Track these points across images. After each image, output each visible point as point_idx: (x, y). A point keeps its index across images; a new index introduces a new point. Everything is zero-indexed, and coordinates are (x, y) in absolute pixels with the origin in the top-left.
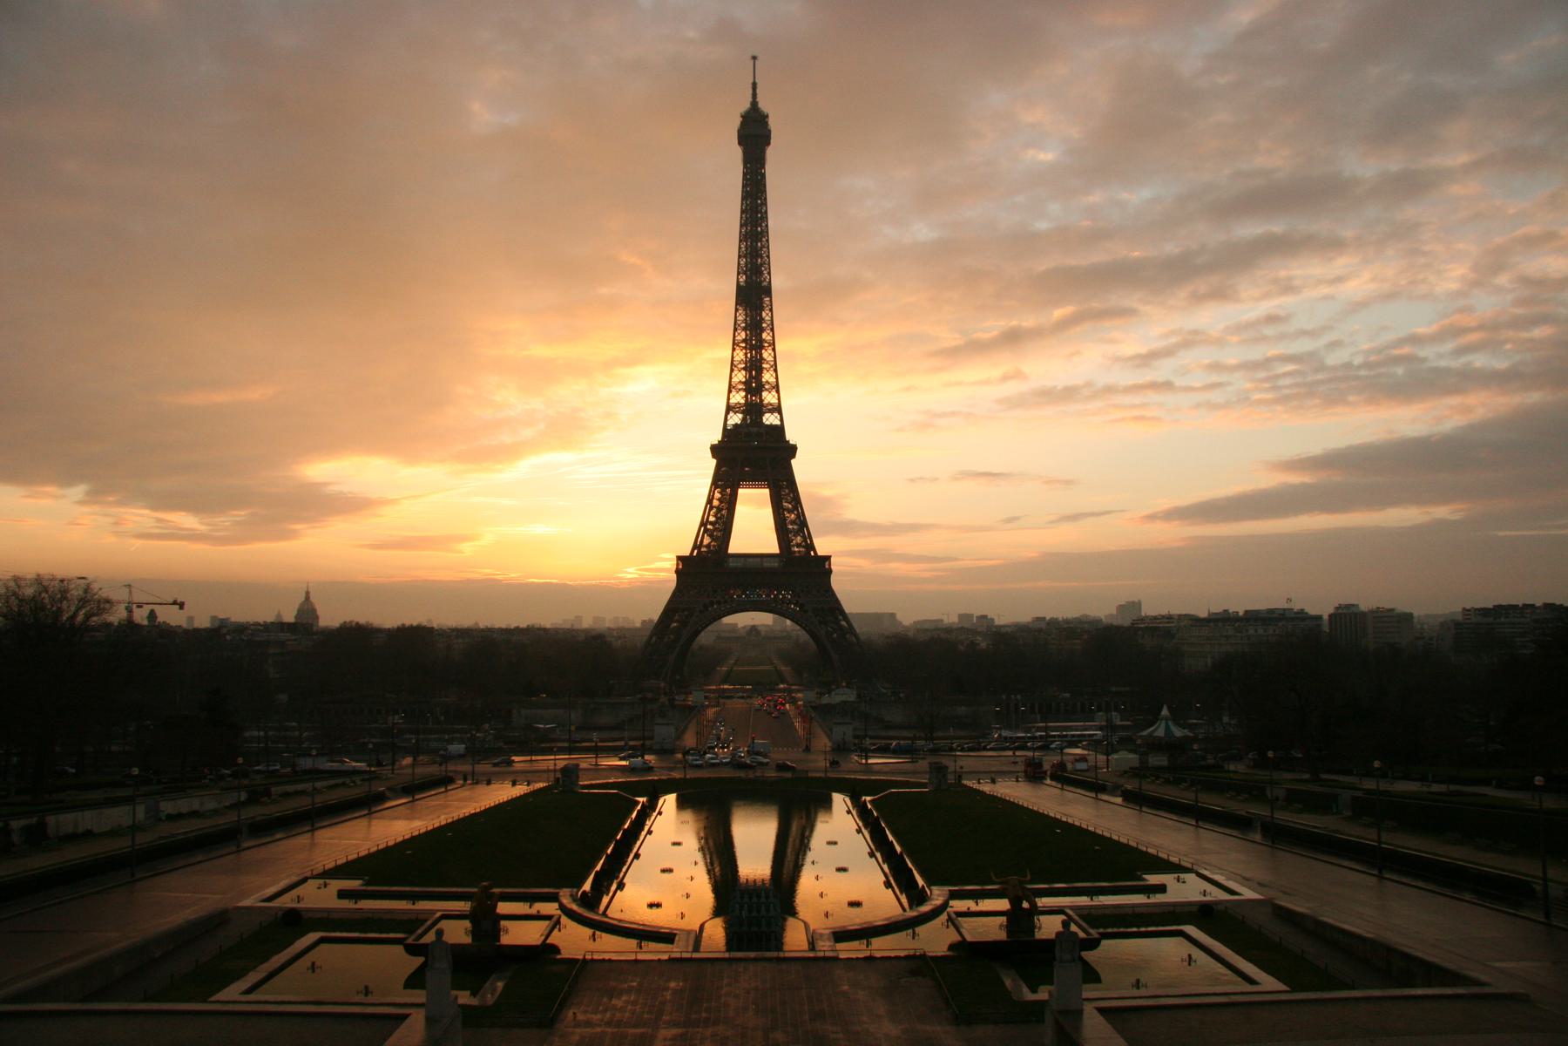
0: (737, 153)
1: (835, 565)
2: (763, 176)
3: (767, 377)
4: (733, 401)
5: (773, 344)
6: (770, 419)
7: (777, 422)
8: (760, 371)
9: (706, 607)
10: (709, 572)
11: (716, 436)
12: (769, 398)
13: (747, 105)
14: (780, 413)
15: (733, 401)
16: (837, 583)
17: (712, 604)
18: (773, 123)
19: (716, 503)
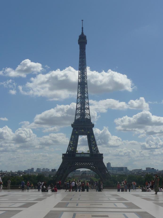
0: (78, 46)
2: (85, 52)
3: (86, 106)
4: (77, 112)
5: (88, 97)
6: (87, 117)
7: (89, 118)
8: (84, 104)
10: (71, 158)
11: (73, 122)
12: (87, 111)
13: (81, 34)
14: (90, 115)
15: (77, 112)
16: (105, 161)
18: (87, 38)
19: (73, 139)
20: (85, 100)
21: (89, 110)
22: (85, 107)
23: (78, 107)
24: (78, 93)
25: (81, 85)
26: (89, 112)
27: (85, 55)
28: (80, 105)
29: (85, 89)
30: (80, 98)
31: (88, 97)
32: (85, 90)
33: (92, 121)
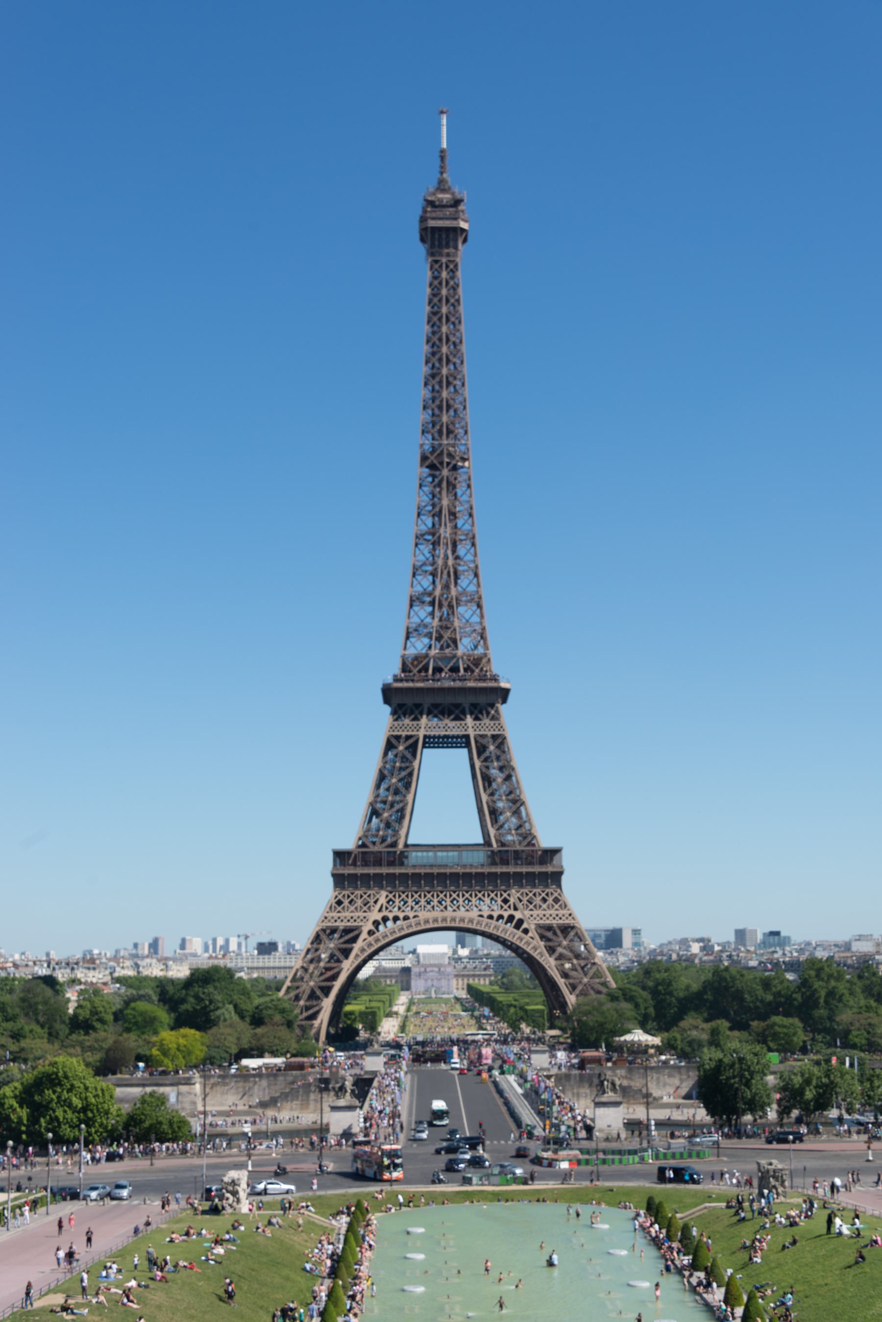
1: (567, 861)
4: (415, 620)
9: (376, 924)
11: (389, 670)
13: (432, 186)
17: (385, 919)
20: (454, 551)
21: (479, 606)
22: (460, 589)
23: (419, 589)
24: (419, 515)
25: (432, 467)
26: (482, 616)
27: (458, 301)
28: (430, 578)
29: (454, 487)
30: (433, 544)
31: (474, 537)
32: (459, 492)
33: (497, 667)
